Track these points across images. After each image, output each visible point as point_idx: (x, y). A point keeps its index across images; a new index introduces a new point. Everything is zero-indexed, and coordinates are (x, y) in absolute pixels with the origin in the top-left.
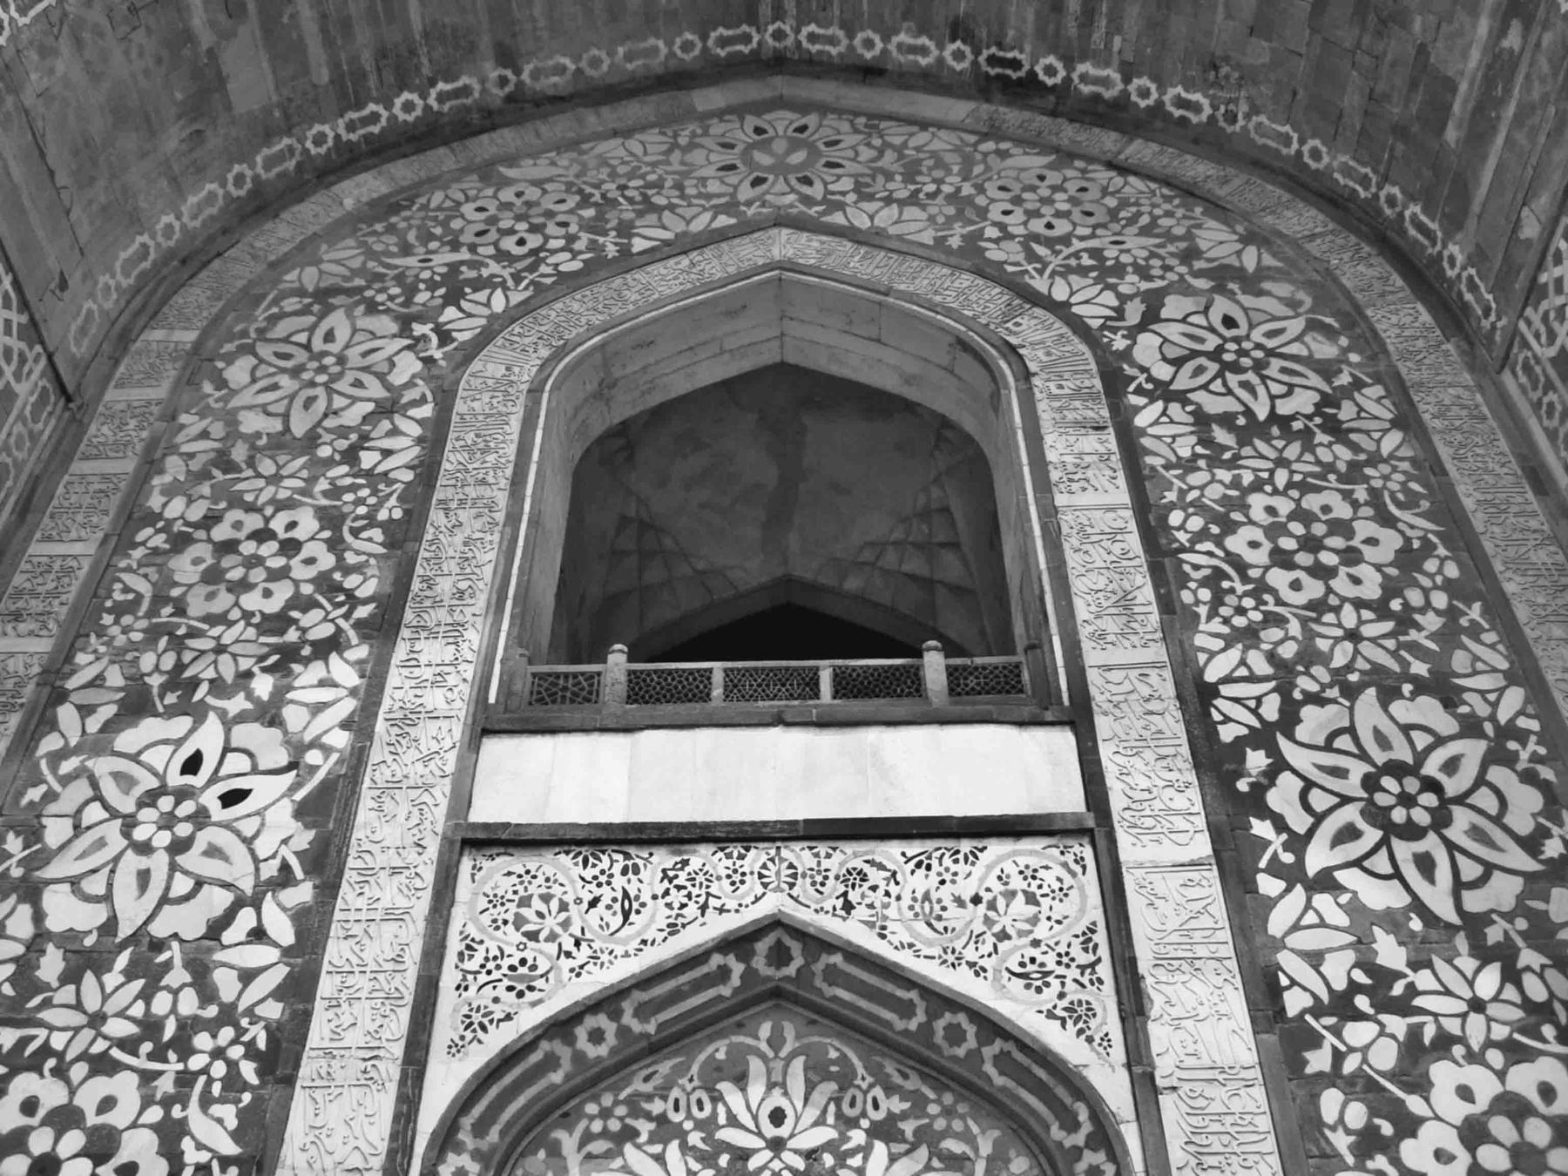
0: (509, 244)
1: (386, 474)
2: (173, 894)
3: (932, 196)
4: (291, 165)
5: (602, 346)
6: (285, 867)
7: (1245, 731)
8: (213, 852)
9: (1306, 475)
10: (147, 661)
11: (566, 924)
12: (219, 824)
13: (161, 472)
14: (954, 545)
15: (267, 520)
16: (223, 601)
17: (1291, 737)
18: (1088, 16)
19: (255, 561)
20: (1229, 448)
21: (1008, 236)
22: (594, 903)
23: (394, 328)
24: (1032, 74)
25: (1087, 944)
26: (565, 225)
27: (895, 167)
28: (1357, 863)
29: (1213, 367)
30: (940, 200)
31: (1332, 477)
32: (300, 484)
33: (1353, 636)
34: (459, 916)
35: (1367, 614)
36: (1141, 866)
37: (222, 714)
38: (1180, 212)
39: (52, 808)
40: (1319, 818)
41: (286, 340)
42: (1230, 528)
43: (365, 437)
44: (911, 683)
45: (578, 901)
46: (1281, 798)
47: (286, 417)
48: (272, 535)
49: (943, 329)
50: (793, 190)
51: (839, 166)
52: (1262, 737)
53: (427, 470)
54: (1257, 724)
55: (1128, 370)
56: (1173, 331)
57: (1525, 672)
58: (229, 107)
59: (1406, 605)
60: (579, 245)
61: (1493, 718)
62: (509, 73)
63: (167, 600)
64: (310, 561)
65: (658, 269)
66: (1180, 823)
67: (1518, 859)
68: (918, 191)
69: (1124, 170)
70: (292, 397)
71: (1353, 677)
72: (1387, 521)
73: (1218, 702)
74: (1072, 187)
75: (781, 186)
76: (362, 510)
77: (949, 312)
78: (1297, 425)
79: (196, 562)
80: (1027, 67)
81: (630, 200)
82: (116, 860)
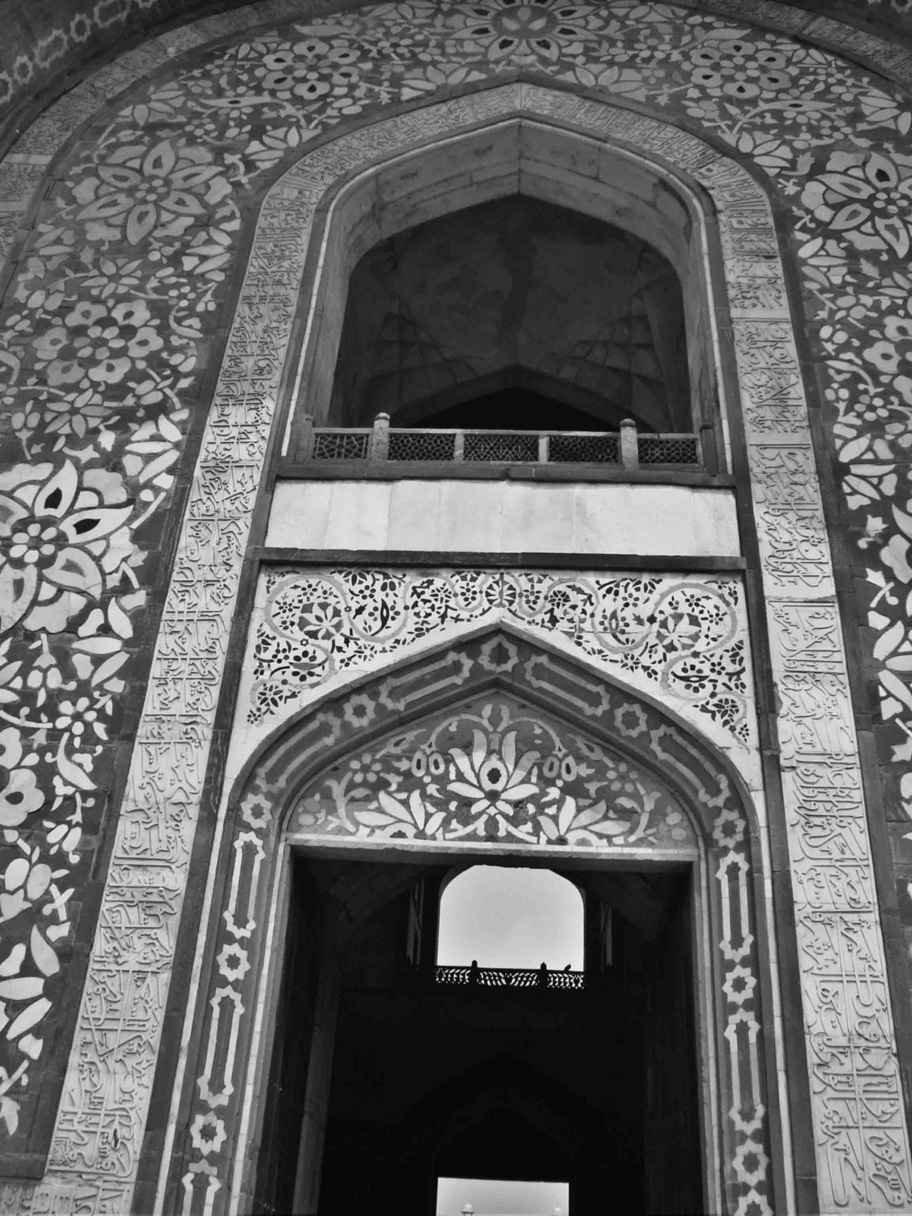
0: (302, 90)
1: (202, 275)
2: (41, 598)
3: (644, 60)
5: (376, 176)
6: (125, 579)
7: (866, 502)
8: (71, 567)
10: (18, 420)
11: (338, 626)
12: (75, 546)
13: (25, 270)
14: (649, 346)
15: (110, 310)
16: (76, 373)
17: (903, 509)
19: (100, 342)
20: (871, 278)
21: (705, 96)
22: (360, 611)
23: (209, 157)
25: (735, 656)
26: (347, 75)
27: (619, 35)
29: (866, 212)
30: (653, 64)
32: (135, 282)
34: (257, 618)
36: (780, 600)
37: (76, 462)
38: (850, 82)
41: (123, 165)
42: (868, 342)
43: (186, 245)
44: (608, 451)
46: (893, 554)
47: (123, 228)
49: (648, 171)
50: (533, 52)
52: (881, 507)
53: (235, 272)
54: (877, 497)
55: (797, 212)
56: (834, 181)
60: (358, 93)
64: (143, 343)
65: (422, 114)
66: (812, 569)
68: (636, 56)
69: (807, 44)
70: (129, 212)
73: (848, 478)
74: (762, 57)
75: (524, 48)
76: (184, 303)
77: (654, 158)
79: (54, 342)
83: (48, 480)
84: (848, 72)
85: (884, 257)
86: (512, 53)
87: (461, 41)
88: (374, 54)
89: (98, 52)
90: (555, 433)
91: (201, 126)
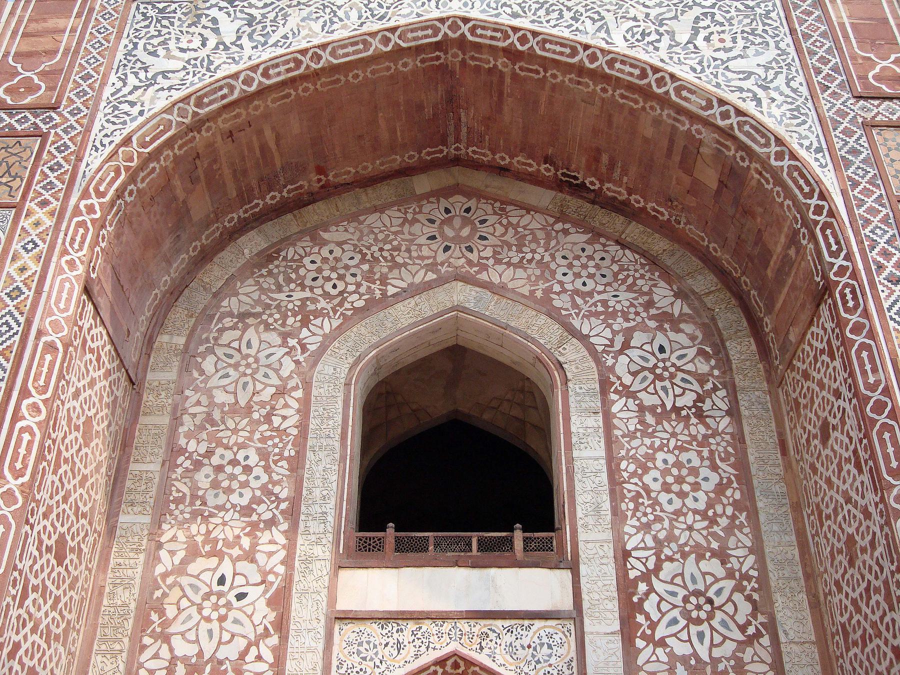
0: (328, 287)
3: (530, 261)
4: (218, 234)
5: (376, 356)
6: (266, 628)
8: (236, 621)
9: (683, 442)
10: (194, 528)
11: (376, 654)
13: (182, 425)
14: (536, 408)
17: (657, 577)
18: (612, 166)
19: (232, 477)
20: (650, 426)
21: (564, 291)
22: (386, 645)
23: (279, 341)
24: (583, 184)
25: (569, 667)
26: (354, 275)
27: (513, 241)
28: (675, 635)
29: (651, 377)
30: (533, 265)
31: (694, 443)
32: (247, 434)
33: (690, 528)
34: (336, 649)
35: (698, 517)
37: (231, 556)
38: (648, 275)
39: (167, 600)
40: (663, 614)
41: (228, 345)
42: (646, 470)
43: (273, 408)
45: (381, 644)
46: (650, 605)
47: (235, 393)
48: (239, 463)
49: (532, 351)
51: (485, 238)
52: (646, 577)
53: (303, 427)
56: (634, 354)
57: (757, 549)
58: (190, 219)
59: (715, 513)
60: (362, 290)
61: (740, 570)
63: (197, 497)
64: (257, 478)
67: (738, 635)
68: (523, 258)
69: (624, 246)
70: (237, 382)
71: (687, 549)
72: (714, 468)
74: (597, 256)
75: (457, 253)
76: (277, 450)
77: (534, 341)
78: (684, 413)
81: (385, 258)
82: (198, 624)
83: (217, 568)
84: (647, 268)
85: (659, 410)
86: (451, 257)
87: (420, 246)
88: (369, 257)
89: (205, 257)
91: (271, 315)
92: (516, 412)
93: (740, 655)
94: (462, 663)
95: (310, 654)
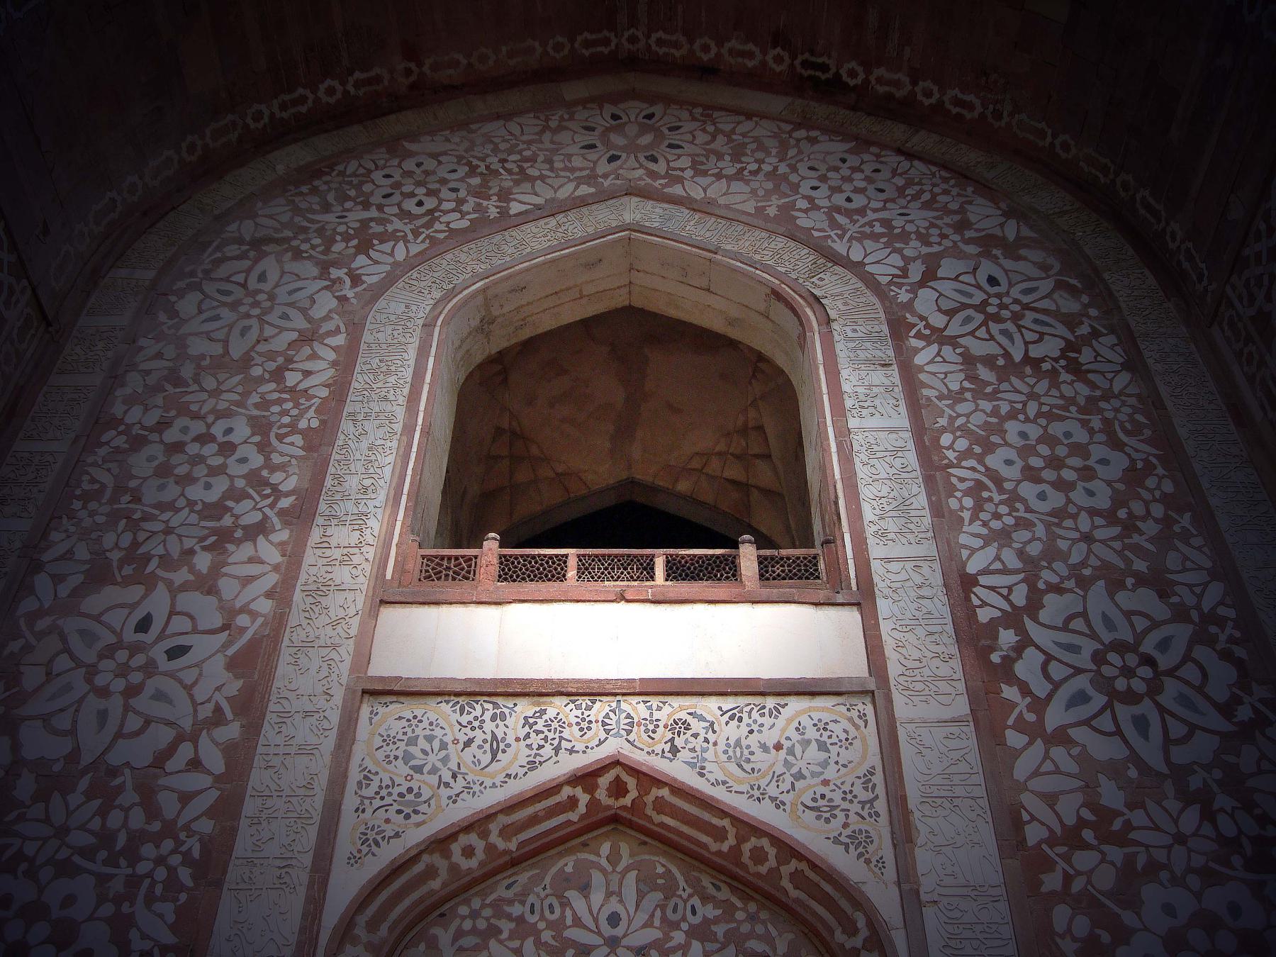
0: (410, 205)
3: (752, 173)
5: (484, 290)
8: (160, 696)
9: (1052, 406)
10: (109, 539)
11: (445, 760)
12: (165, 674)
13: (123, 385)
14: (767, 457)
15: (209, 426)
17: (1035, 619)
22: (468, 743)
23: (315, 271)
27: (725, 149)
28: (1086, 722)
29: (980, 318)
30: (760, 177)
31: (1073, 409)
32: (237, 397)
33: (1087, 538)
35: (1099, 521)
37: (169, 584)
38: (955, 191)
40: (1057, 686)
42: (989, 448)
43: (290, 360)
45: (455, 742)
46: (1027, 667)
47: (226, 342)
48: (212, 439)
49: (761, 282)
51: (679, 147)
52: (1012, 618)
53: (340, 390)
56: (947, 287)
59: (1130, 514)
60: (465, 208)
61: (1198, 607)
62: (413, 66)
64: (243, 460)
65: (530, 228)
68: (744, 169)
69: (910, 156)
71: (1087, 572)
72: (1117, 445)
74: (868, 169)
75: (632, 162)
76: (286, 420)
77: (766, 268)
78: (1046, 366)
80: (833, 70)
81: (509, 172)
82: (81, 700)
83: (138, 603)
90: (672, 551)
92: (734, 472)
93: (1231, 759)
94: (631, 783)
95: (305, 759)
